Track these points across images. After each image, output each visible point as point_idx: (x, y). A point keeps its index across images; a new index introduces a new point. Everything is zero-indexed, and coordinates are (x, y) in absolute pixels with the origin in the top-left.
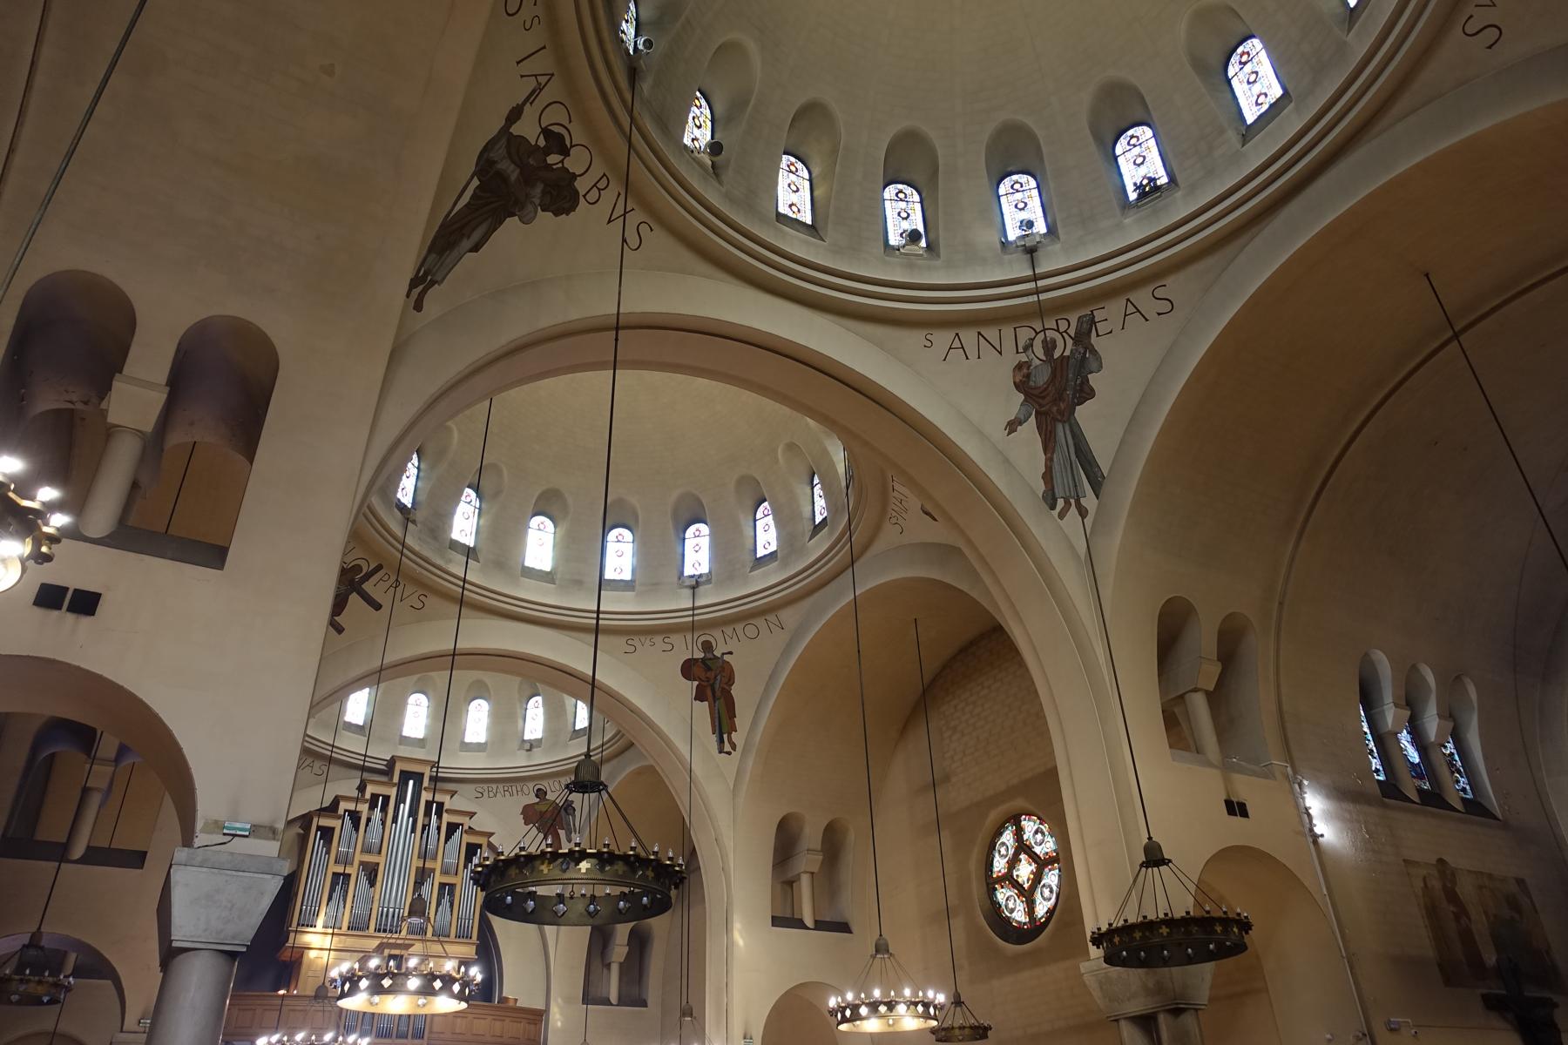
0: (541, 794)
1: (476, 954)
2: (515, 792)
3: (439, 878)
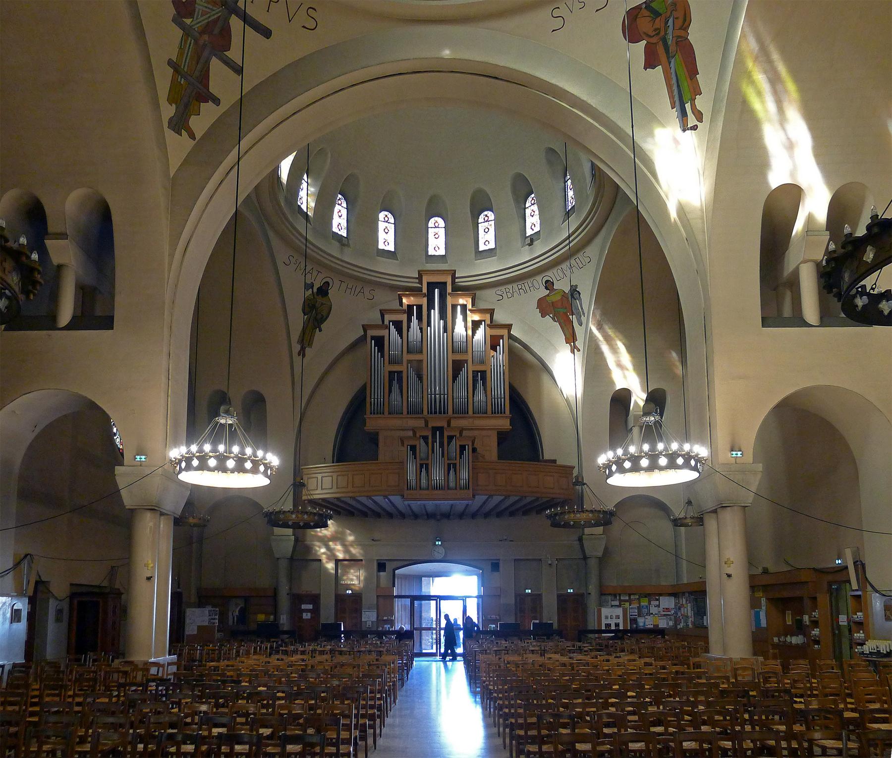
0: (549, 285)
3: (471, 368)
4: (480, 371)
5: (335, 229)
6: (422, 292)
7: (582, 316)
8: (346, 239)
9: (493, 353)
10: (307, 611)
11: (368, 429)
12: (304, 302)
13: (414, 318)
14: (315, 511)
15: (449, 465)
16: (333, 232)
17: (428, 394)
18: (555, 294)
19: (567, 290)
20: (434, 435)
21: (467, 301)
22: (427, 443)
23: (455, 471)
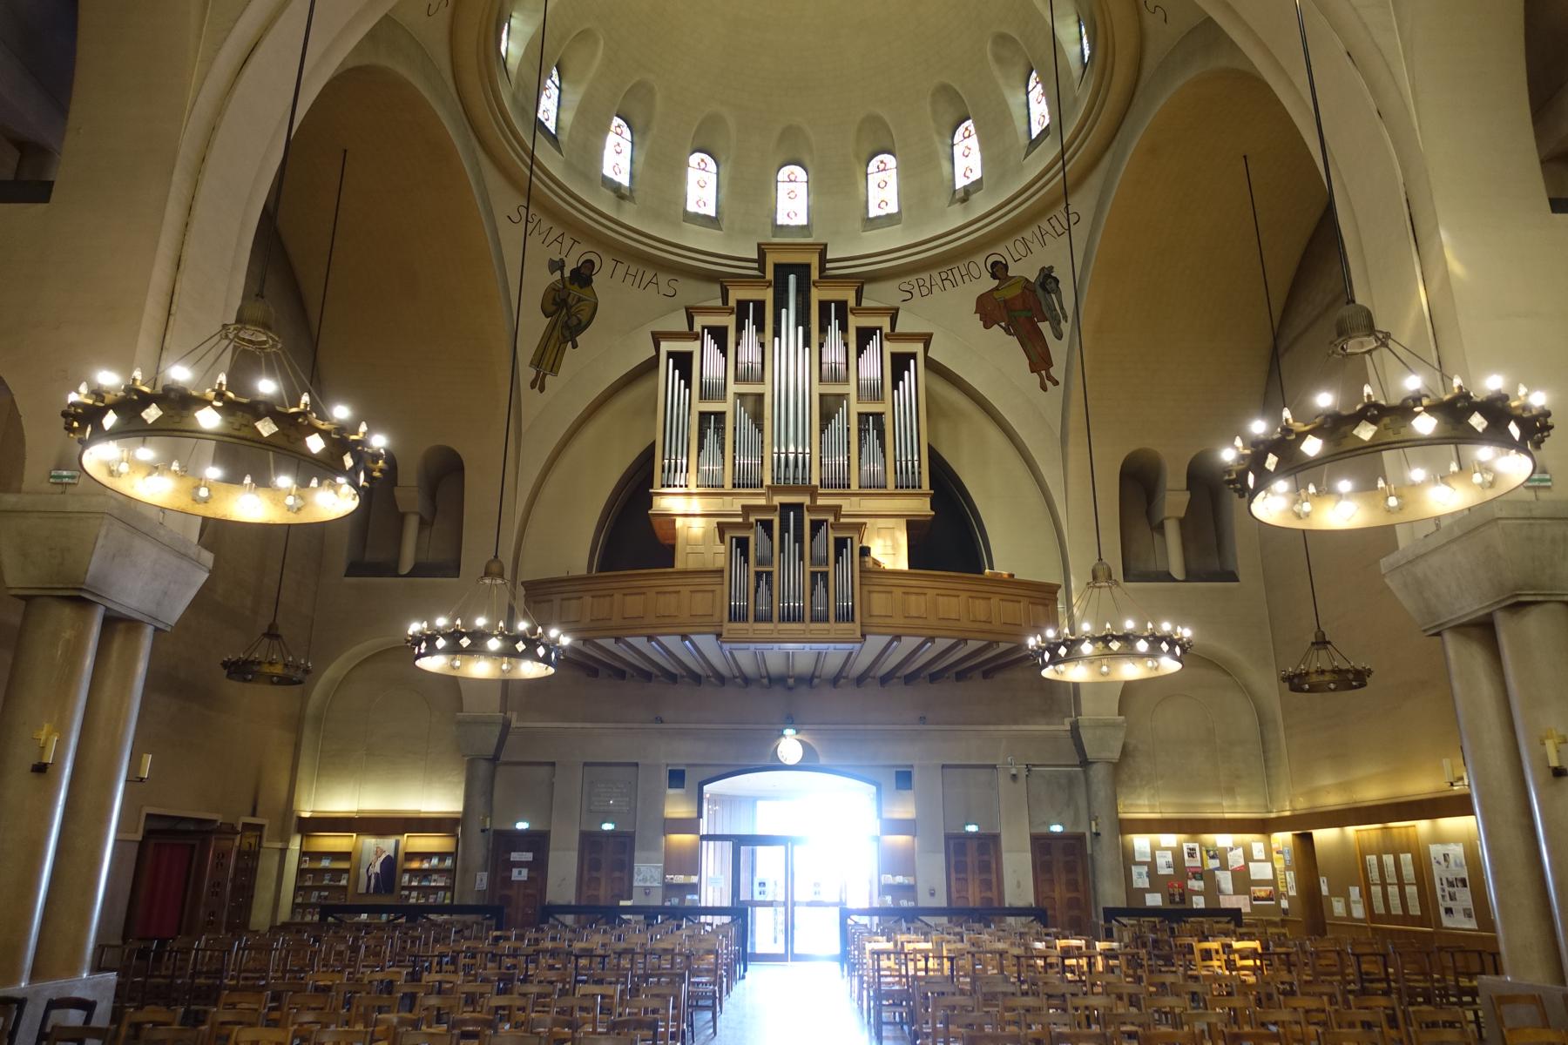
0: (998, 270)
1: (932, 509)
3: (856, 408)
4: (872, 414)
5: (608, 171)
7: (1063, 322)
10: (520, 864)
16: (604, 176)
17: (773, 453)
18: (1009, 286)
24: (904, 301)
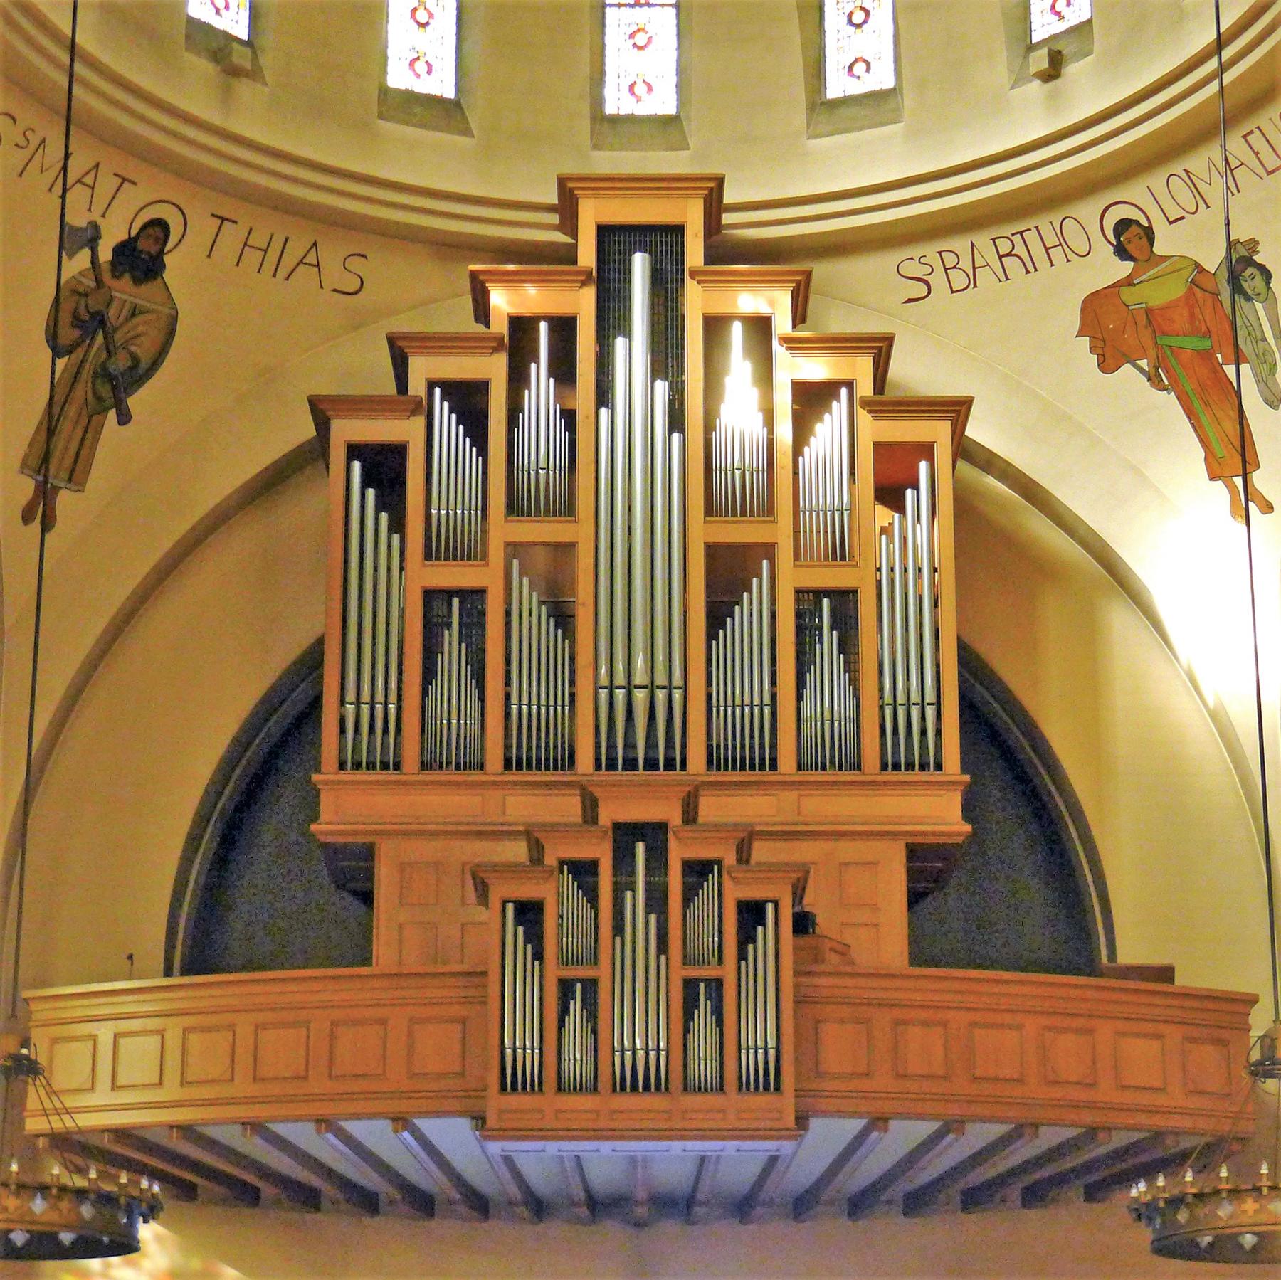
2: (1038, 251)
3: (790, 577)
6: (575, 262)
8: (248, 51)
9: (884, 515)
11: (322, 833)
12: (57, 302)
13: (540, 371)
14: (80, 1182)
15: (690, 986)
17: (597, 688)
19: (1213, 258)
20: (623, 858)
21: (772, 303)
22: (592, 896)
23: (718, 1012)
24: (909, 301)
